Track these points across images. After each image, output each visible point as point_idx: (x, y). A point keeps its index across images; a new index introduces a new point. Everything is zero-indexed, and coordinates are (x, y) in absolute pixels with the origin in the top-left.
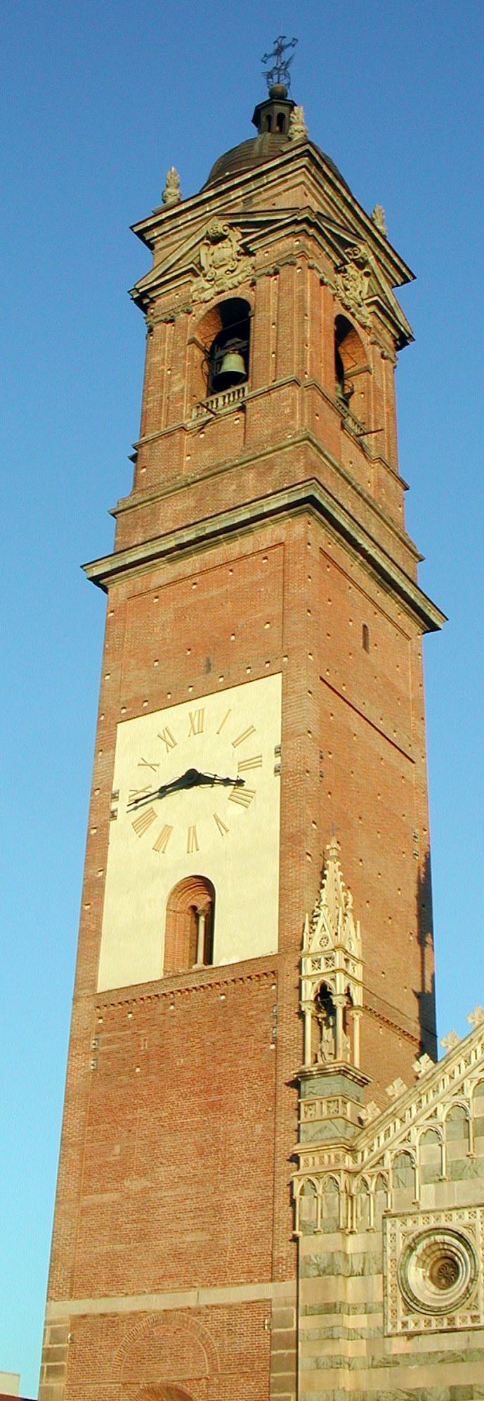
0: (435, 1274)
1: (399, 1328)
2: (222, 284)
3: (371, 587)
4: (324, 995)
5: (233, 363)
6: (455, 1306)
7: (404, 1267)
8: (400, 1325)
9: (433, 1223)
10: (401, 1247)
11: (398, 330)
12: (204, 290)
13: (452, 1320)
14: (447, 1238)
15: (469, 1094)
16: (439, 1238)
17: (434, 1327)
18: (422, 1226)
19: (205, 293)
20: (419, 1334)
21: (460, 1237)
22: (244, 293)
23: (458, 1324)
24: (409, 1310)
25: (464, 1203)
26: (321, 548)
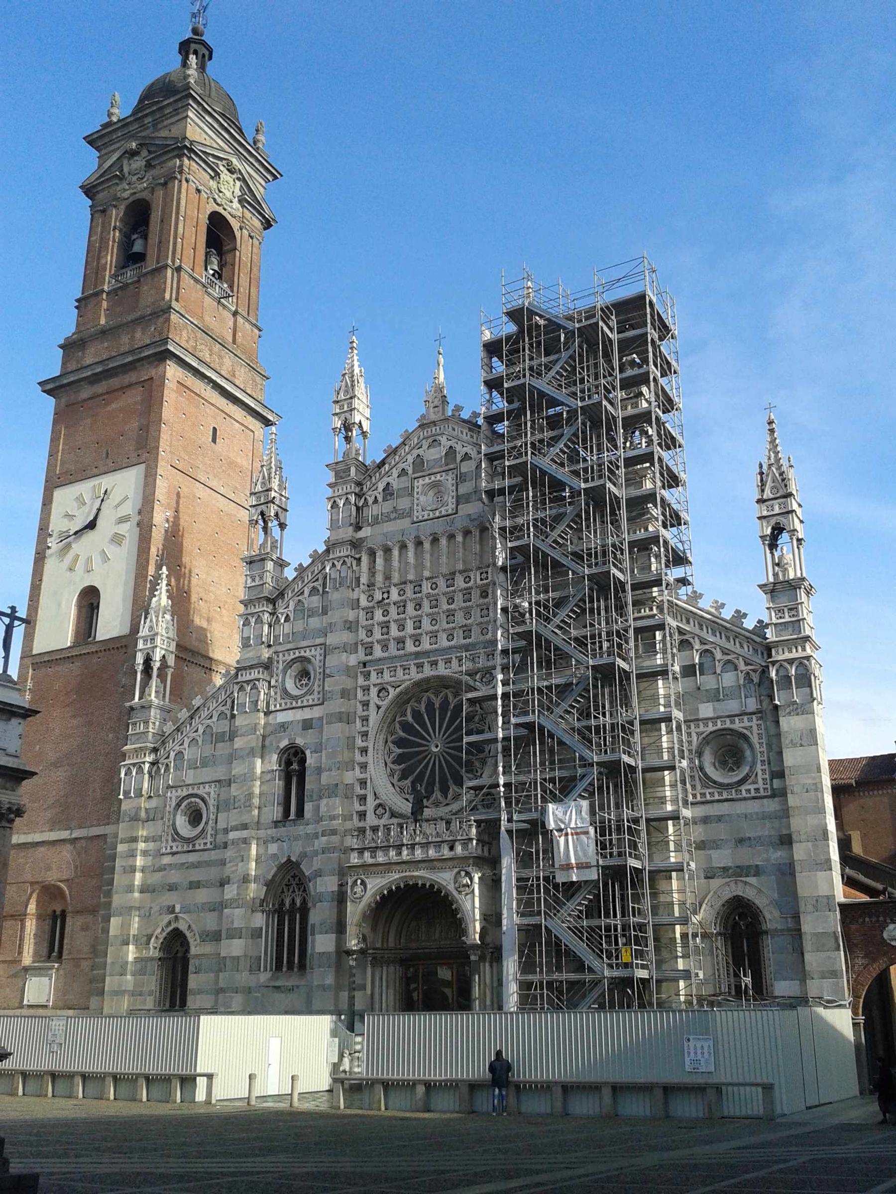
0: (192, 818)
1: (169, 850)
2: (135, 188)
3: (222, 402)
4: (148, 661)
5: (138, 247)
6: (197, 837)
7: (174, 816)
8: (169, 848)
9: (191, 791)
10: (174, 804)
11: (264, 217)
12: (125, 190)
13: (194, 845)
14: (198, 800)
15: (215, 719)
16: (193, 800)
17: (185, 848)
18: (185, 793)
19: (125, 192)
20: (177, 853)
21: (203, 799)
22: (145, 195)
23: (197, 847)
24: (174, 840)
25: (207, 780)
26: (178, 382)
